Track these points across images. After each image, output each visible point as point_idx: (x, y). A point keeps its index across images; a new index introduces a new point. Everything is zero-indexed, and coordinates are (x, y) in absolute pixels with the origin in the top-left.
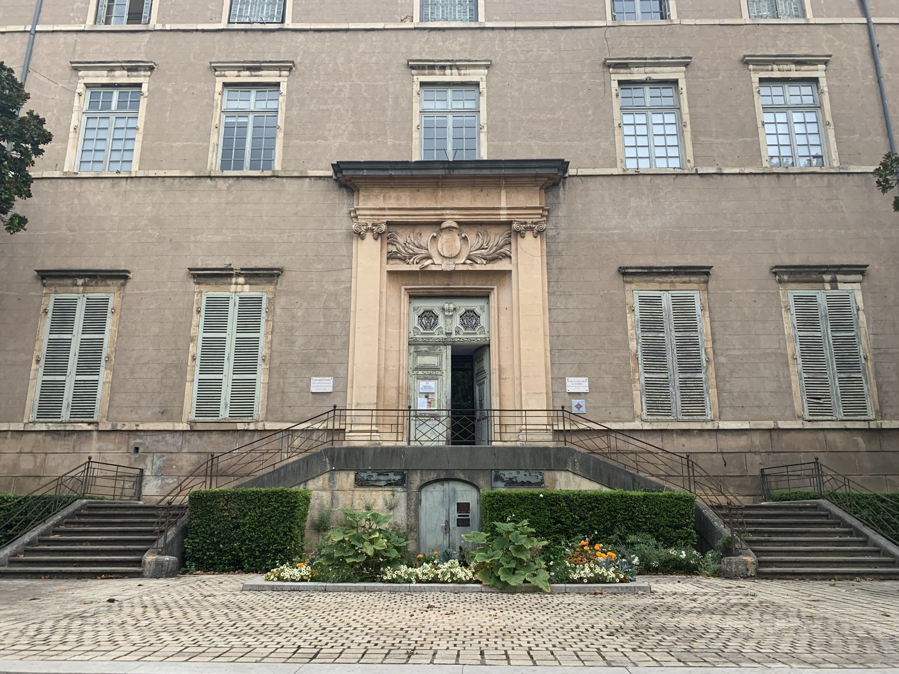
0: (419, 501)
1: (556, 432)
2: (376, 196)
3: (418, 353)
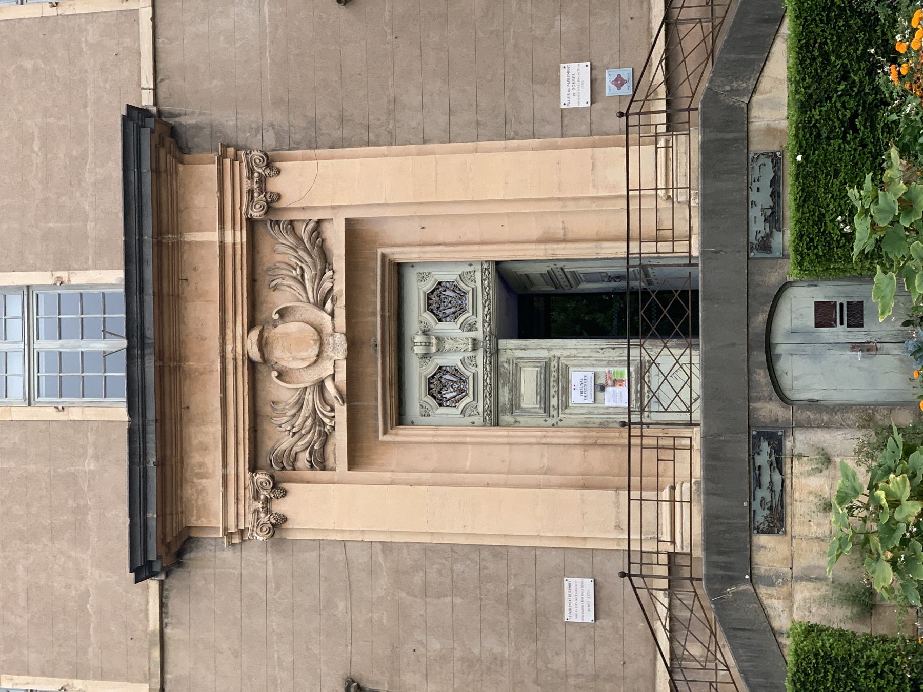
0: (812, 404)
1: (671, 126)
2: (199, 492)
3: (514, 406)
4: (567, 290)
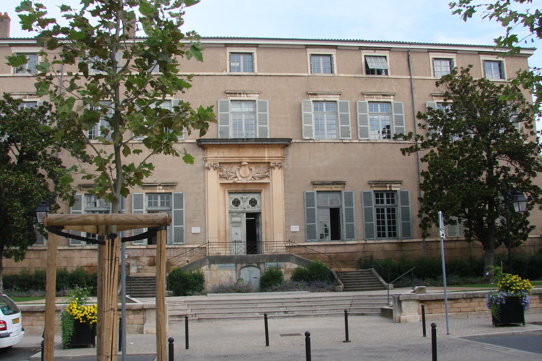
1: (286, 246)
3: (233, 216)
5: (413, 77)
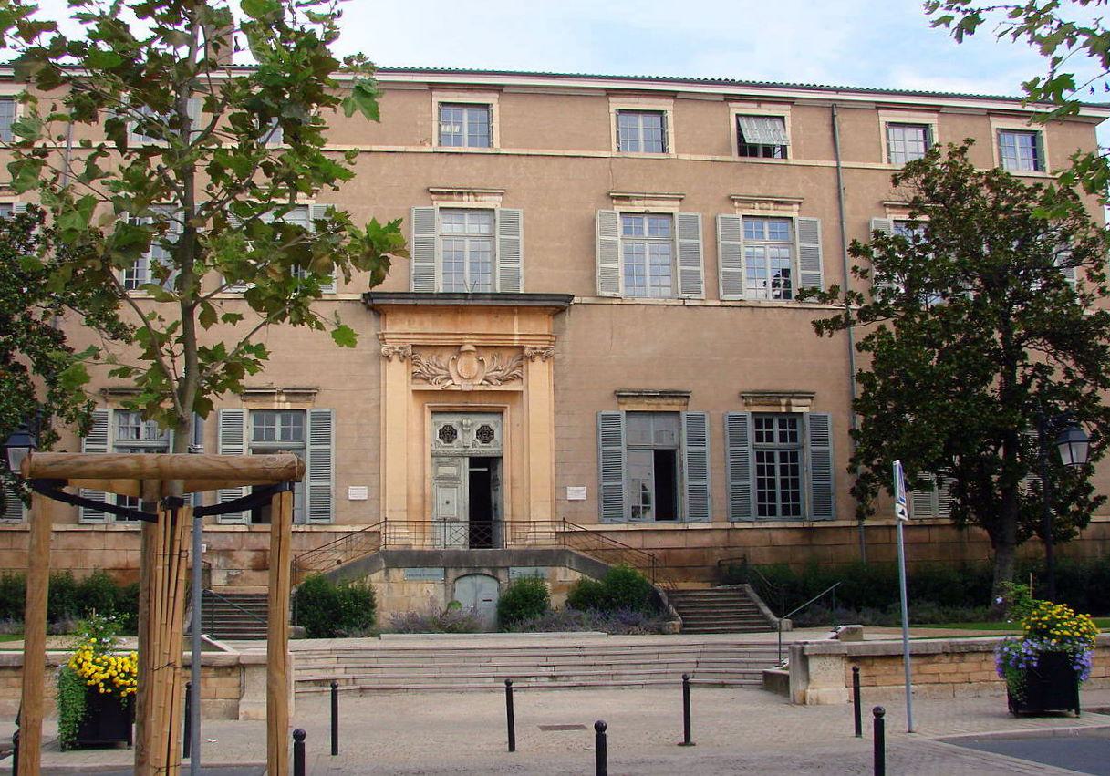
2: (401, 320)
3: (440, 464)
4: (492, 485)
5: (843, 164)
